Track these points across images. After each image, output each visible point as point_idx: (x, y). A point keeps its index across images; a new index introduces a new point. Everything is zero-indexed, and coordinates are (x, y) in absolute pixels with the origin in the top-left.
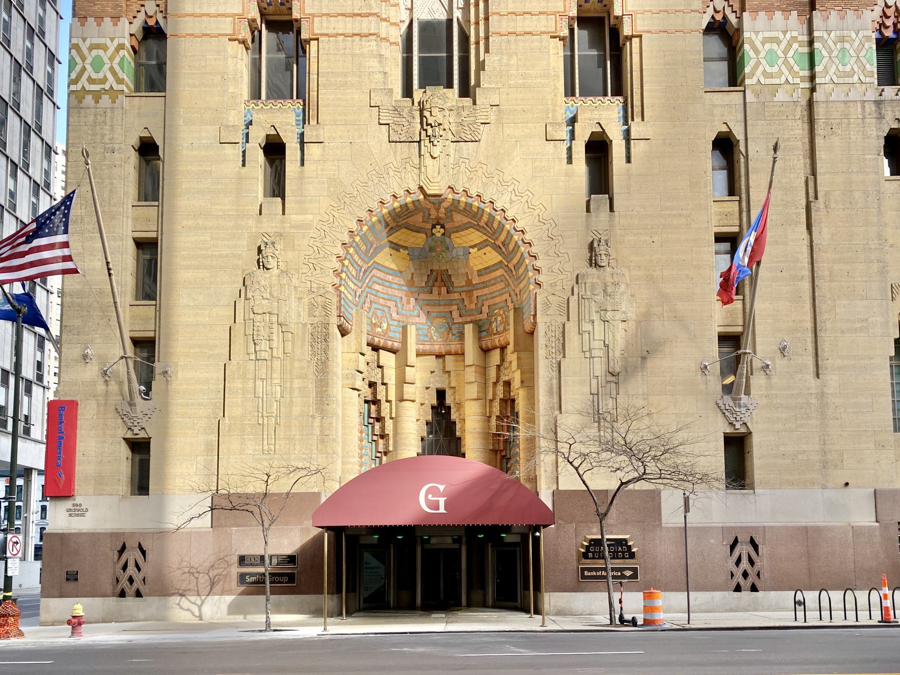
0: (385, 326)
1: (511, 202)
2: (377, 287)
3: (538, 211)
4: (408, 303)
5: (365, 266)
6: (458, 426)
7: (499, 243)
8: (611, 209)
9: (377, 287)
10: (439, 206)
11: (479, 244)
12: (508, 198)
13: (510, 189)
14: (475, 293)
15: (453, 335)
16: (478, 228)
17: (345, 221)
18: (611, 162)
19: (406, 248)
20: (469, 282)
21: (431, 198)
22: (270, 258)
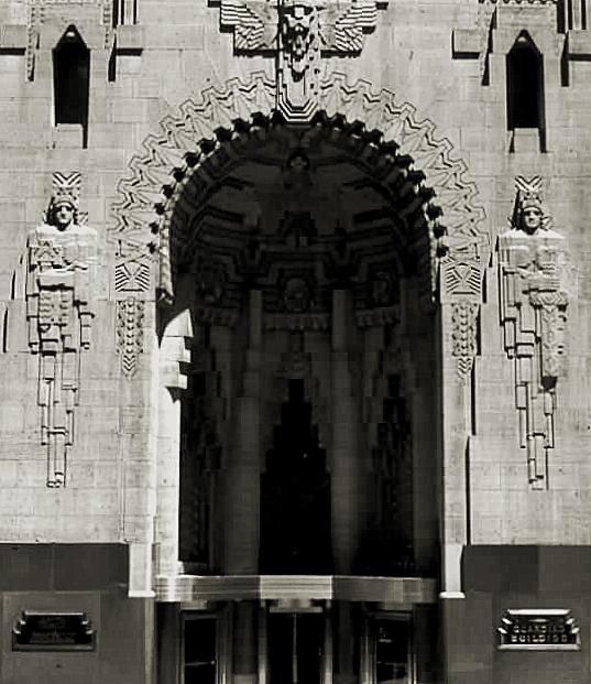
0: (218, 292)
1: (404, 134)
2: (208, 238)
3: (441, 149)
4: (252, 256)
5: (193, 213)
6: (321, 435)
7: (383, 184)
8: (543, 149)
9: (208, 238)
10: (303, 134)
11: (356, 182)
12: (400, 131)
13: (403, 117)
14: (350, 246)
15: (315, 303)
16: (356, 163)
17: (171, 158)
18: (543, 95)
19: (251, 185)
20: (340, 231)
21: (291, 126)
22: (64, 211)
